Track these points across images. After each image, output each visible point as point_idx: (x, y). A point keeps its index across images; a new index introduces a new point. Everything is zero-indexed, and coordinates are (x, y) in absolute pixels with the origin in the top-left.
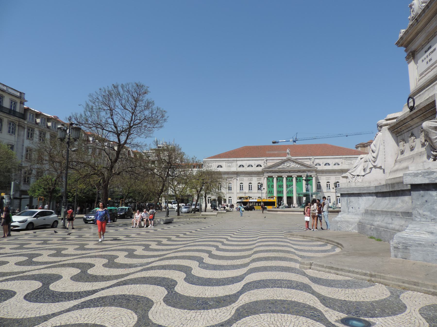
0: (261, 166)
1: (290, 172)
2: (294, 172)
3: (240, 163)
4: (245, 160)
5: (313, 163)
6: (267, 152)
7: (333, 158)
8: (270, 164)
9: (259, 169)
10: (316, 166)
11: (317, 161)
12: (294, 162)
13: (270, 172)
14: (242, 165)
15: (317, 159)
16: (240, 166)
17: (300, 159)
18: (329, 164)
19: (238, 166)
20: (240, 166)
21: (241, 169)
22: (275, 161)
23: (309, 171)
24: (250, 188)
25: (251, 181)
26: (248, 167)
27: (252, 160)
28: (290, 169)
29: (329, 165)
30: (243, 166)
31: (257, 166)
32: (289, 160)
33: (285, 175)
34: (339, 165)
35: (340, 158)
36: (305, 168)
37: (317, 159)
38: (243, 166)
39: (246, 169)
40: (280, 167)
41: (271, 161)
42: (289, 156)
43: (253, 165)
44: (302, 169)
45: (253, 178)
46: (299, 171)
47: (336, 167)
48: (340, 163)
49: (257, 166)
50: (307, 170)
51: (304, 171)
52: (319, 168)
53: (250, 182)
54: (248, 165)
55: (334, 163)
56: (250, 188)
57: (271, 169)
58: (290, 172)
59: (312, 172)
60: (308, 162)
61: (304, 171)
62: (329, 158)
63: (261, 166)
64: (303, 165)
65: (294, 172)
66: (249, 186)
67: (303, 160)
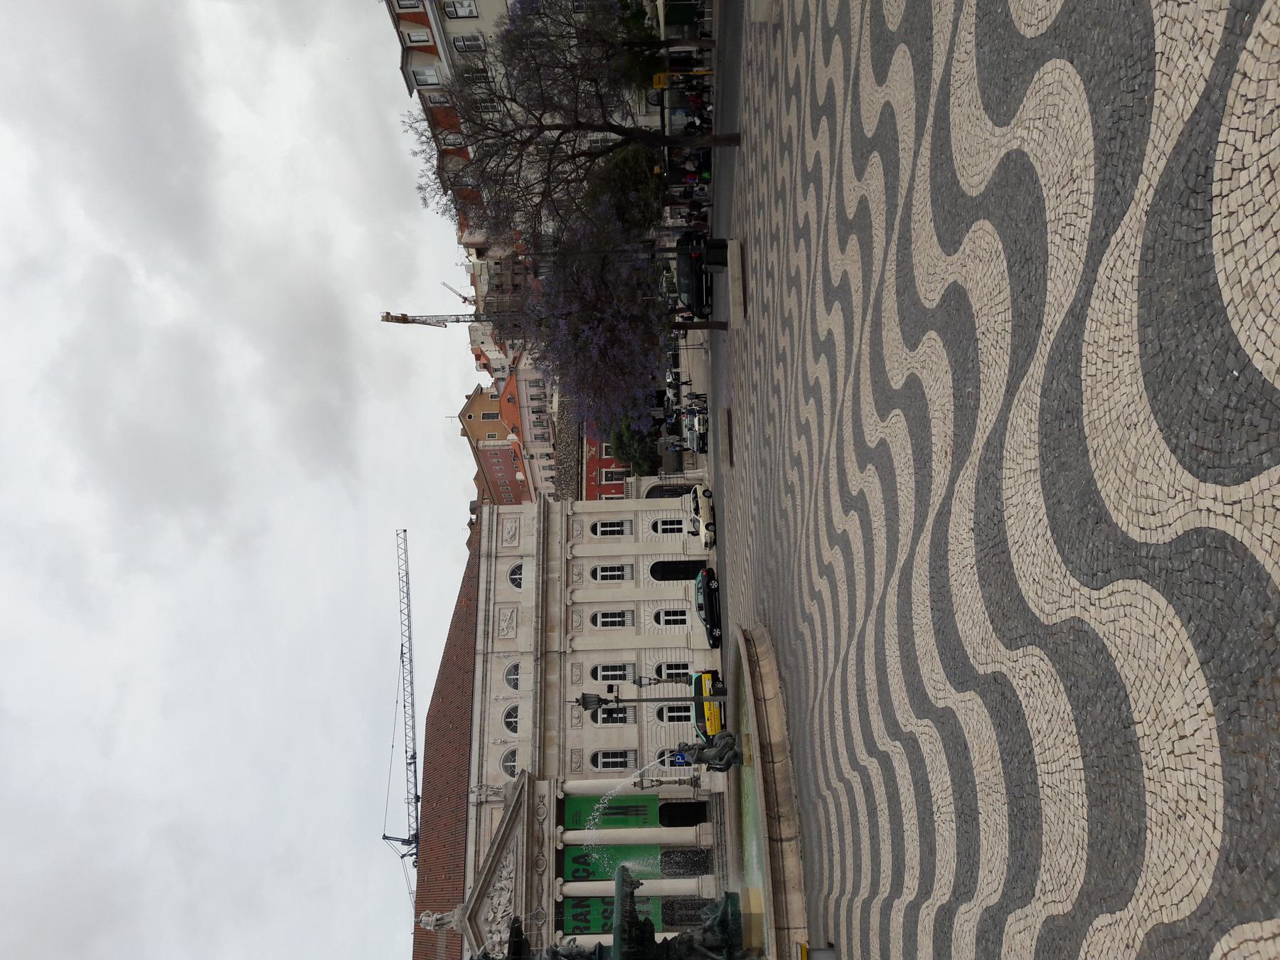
2: (532, 891)
7: (484, 692)
12: (483, 893)
15: (481, 766)
17: (477, 853)
18: (512, 713)
23: (533, 812)
29: (515, 709)
32: (473, 918)
34: (516, 667)
35: (485, 661)
36: (520, 832)
37: (481, 766)
44: (522, 850)
46: (533, 864)
47: (527, 678)
48: (509, 663)
51: (535, 839)
52: (524, 762)
55: (509, 690)
60: (495, 817)
61: (535, 839)
62: (483, 713)
64: (501, 844)
65: (532, 891)
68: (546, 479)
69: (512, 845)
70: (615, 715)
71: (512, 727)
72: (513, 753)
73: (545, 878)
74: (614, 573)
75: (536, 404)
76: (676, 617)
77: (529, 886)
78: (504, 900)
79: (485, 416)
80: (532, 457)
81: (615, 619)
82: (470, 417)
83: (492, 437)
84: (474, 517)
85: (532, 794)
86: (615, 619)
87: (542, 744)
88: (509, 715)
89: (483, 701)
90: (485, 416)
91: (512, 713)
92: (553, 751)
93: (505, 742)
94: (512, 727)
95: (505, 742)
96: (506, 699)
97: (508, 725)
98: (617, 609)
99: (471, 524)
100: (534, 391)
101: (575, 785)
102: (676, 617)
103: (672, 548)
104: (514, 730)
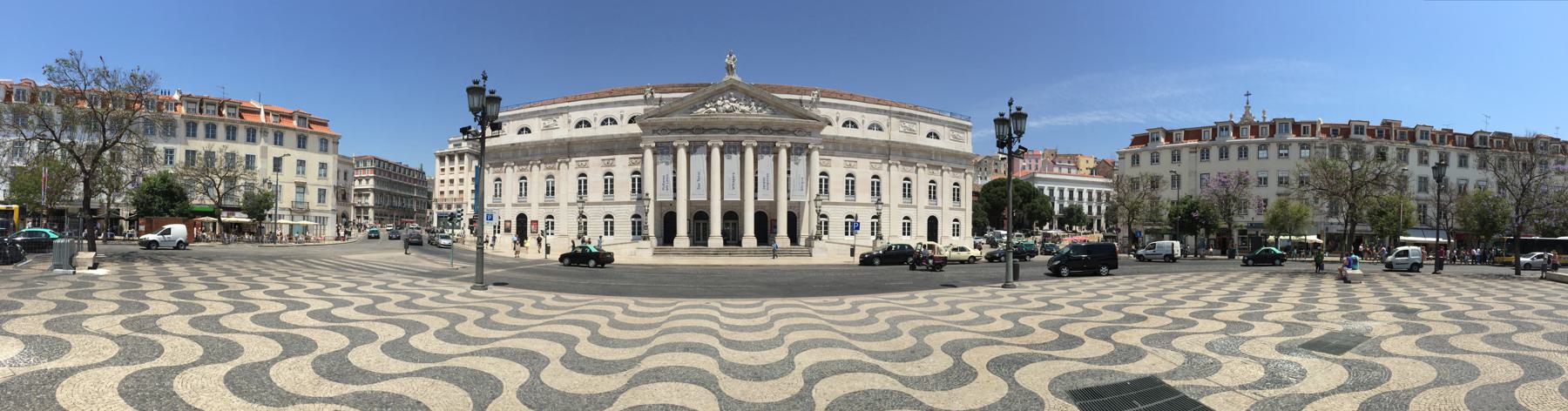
1: (733, 129)
2: (749, 129)
16: (579, 125)
19: (574, 123)
20: (579, 125)
21: (583, 133)
33: (716, 142)
38: (588, 124)
39: (597, 131)
40: (701, 111)
43: (617, 118)
45: (618, 157)
46: (765, 129)
47: (874, 135)
51: (782, 131)
54: (600, 118)
55: (867, 124)
58: (733, 129)
59: (809, 134)
70: (850, 189)
71: (846, 124)
74: (932, 194)
76: (907, 230)
81: (907, 191)
86: (907, 191)
94: (846, 124)
98: (913, 193)
102: (907, 230)
103: (944, 229)
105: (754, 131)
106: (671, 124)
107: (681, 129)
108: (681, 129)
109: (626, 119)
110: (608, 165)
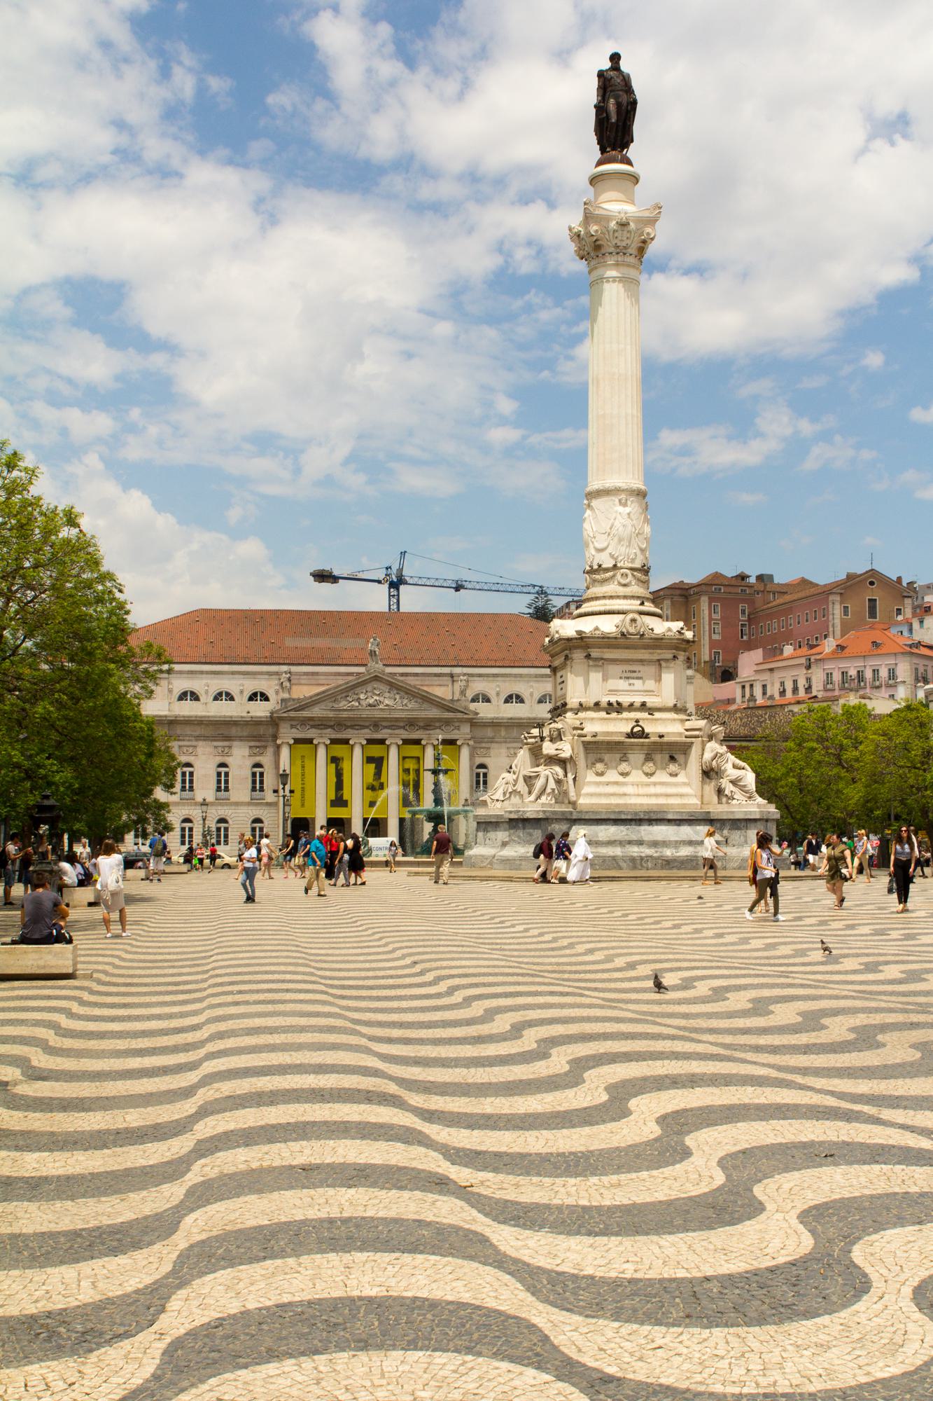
0: (267, 699)
2: (394, 724)
3: (180, 684)
4: (202, 672)
5: (463, 693)
6: (290, 642)
7: (536, 676)
8: (303, 691)
9: (260, 710)
10: (473, 706)
11: (478, 686)
13: (305, 722)
14: (193, 693)
16: (183, 696)
17: (416, 675)
18: (520, 699)
19: (177, 693)
20: (183, 696)
21: (188, 709)
22: (322, 679)
23: (447, 722)
24: (222, 784)
25: (228, 755)
26: (216, 699)
27: (233, 673)
28: (378, 714)
29: (522, 701)
30: (195, 697)
31: (251, 699)
32: (376, 678)
36: (434, 713)
37: (480, 675)
38: (195, 697)
40: (343, 704)
41: (304, 680)
42: (377, 667)
43: (235, 693)
44: (423, 714)
46: (411, 723)
49: (251, 699)
50: (439, 720)
51: (428, 725)
52: (485, 711)
53: (219, 760)
54: (213, 691)
56: (222, 784)
57: (305, 714)
58: (376, 724)
59: (458, 728)
60: (442, 691)
61: (428, 725)
63: (267, 699)
64: (427, 699)
66: (219, 774)
67: (427, 681)
68: (782, 684)
69: (425, 705)
72: (488, 701)
73: (401, 731)
75: (868, 674)
77: (397, 720)
78: (387, 702)
79: (872, 601)
80: (808, 667)
82: (872, 583)
83: (846, 613)
84: (753, 580)
85: (461, 721)
87: (495, 724)
88: (518, 697)
89: (529, 676)
90: (872, 601)
91: (520, 699)
92: (489, 732)
93: (498, 694)
94: (508, 699)
95: (498, 694)
96: (532, 694)
97: (510, 697)
99: (743, 577)
100: (884, 673)
101: (465, 752)
104: (506, 701)
105: (400, 727)
106: (311, 719)
107: (320, 724)
108: (320, 724)
109: (247, 695)
110: (223, 754)
